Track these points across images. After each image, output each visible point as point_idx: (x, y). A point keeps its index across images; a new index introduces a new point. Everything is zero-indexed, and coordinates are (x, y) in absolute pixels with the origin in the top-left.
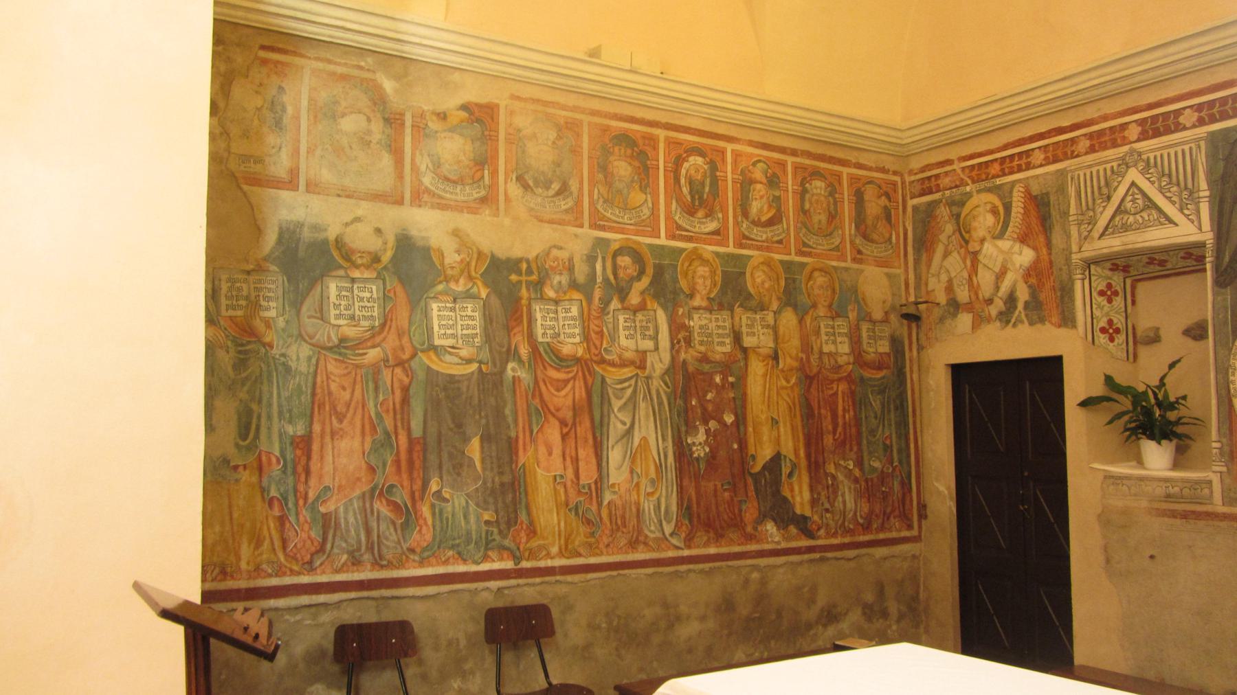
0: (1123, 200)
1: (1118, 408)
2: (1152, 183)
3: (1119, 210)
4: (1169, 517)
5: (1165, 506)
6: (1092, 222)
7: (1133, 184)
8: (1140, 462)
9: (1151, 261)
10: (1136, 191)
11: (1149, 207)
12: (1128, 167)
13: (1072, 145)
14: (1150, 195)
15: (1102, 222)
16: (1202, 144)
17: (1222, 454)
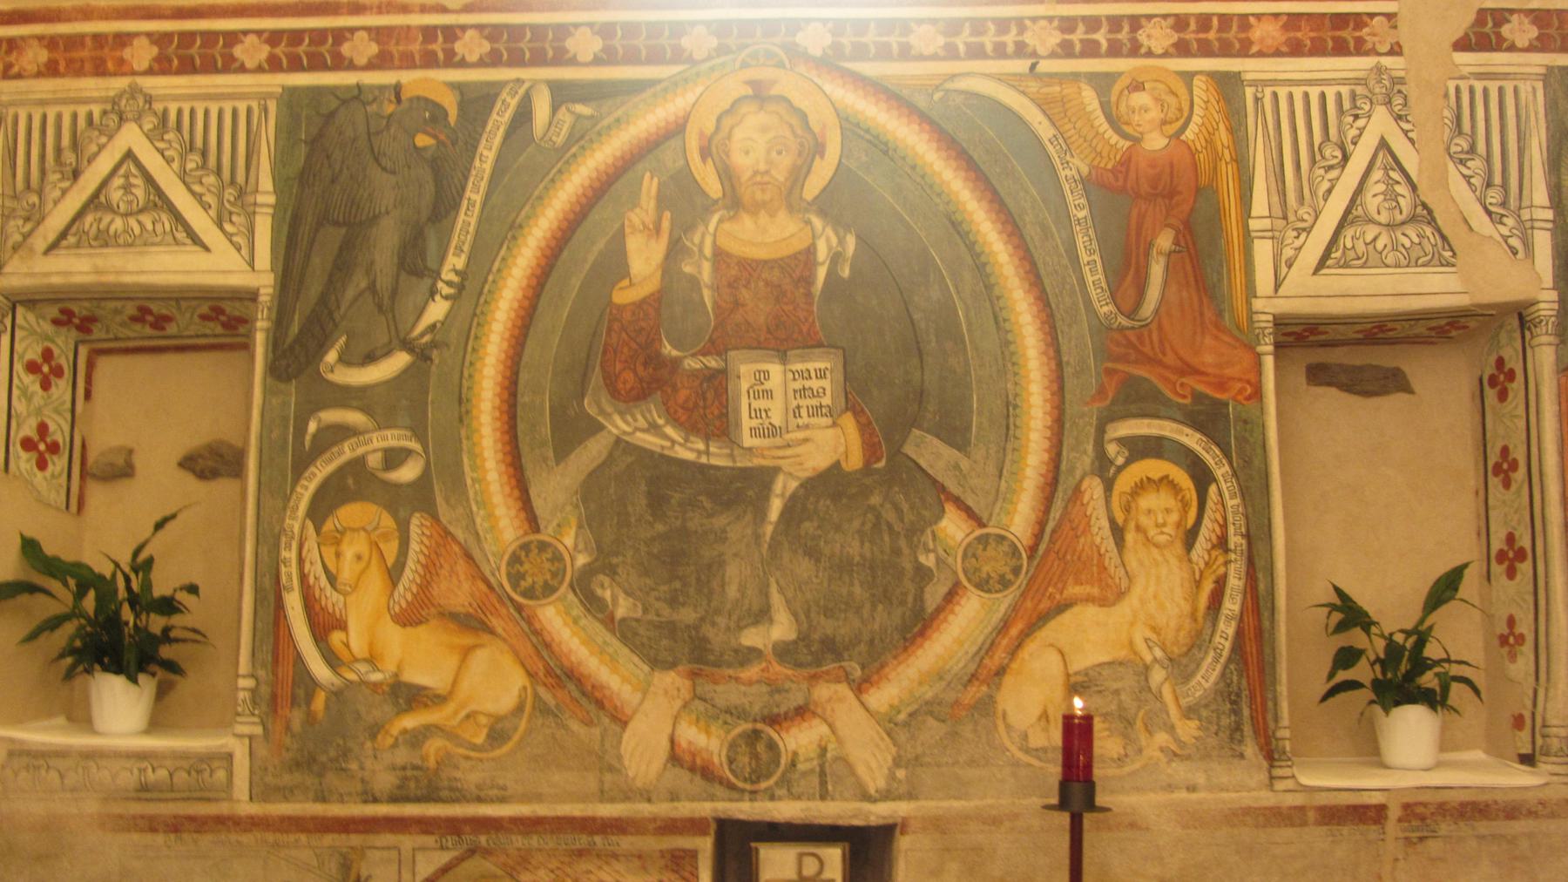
0: (105, 183)
1: (45, 608)
2: (169, 161)
3: (95, 202)
4: (142, 831)
5: (136, 808)
6: (36, 217)
7: (129, 155)
8: (81, 717)
9: (142, 314)
10: (134, 170)
11: (156, 205)
12: (122, 119)
13: (9, 51)
14: (163, 185)
15: (57, 219)
16: (272, 106)
17: (254, 702)
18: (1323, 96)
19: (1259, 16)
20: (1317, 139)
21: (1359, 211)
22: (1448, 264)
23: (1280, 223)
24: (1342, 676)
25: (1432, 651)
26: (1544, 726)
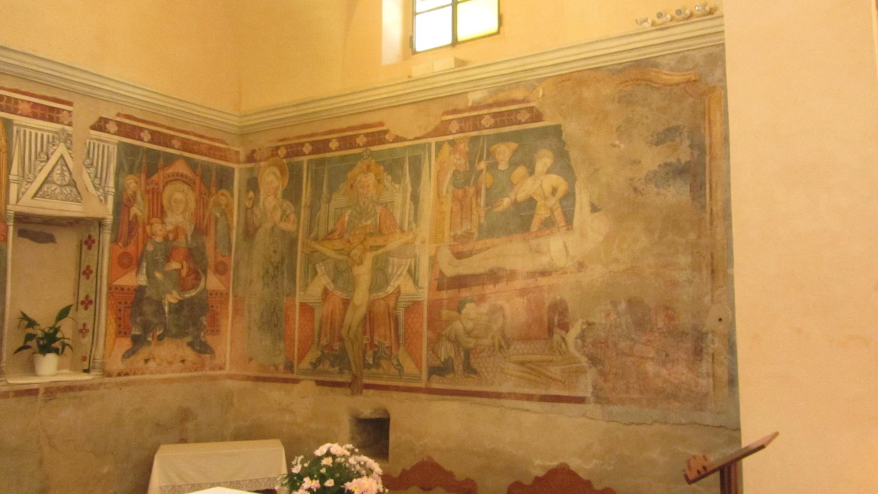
18: (42, 136)
19: (23, 101)
20: (39, 149)
21: (50, 179)
22: (80, 202)
23: (21, 178)
24: (29, 343)
25: (59, 335)
26: (94, 359)
